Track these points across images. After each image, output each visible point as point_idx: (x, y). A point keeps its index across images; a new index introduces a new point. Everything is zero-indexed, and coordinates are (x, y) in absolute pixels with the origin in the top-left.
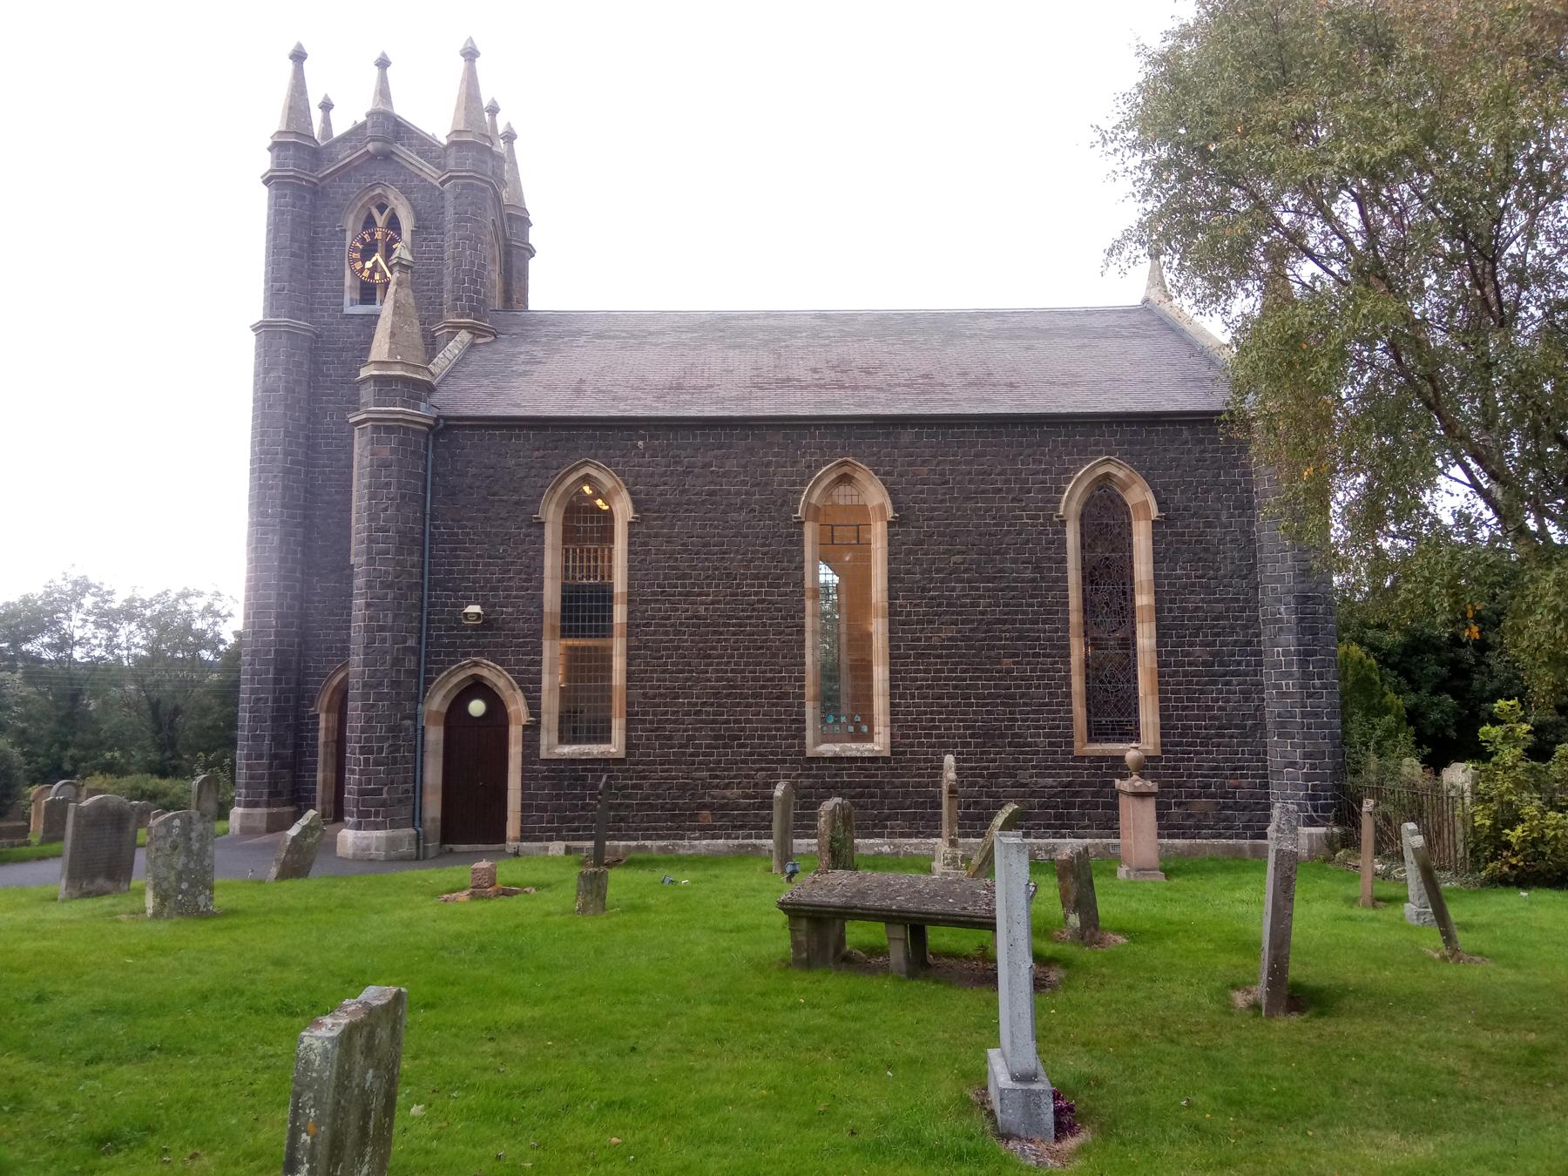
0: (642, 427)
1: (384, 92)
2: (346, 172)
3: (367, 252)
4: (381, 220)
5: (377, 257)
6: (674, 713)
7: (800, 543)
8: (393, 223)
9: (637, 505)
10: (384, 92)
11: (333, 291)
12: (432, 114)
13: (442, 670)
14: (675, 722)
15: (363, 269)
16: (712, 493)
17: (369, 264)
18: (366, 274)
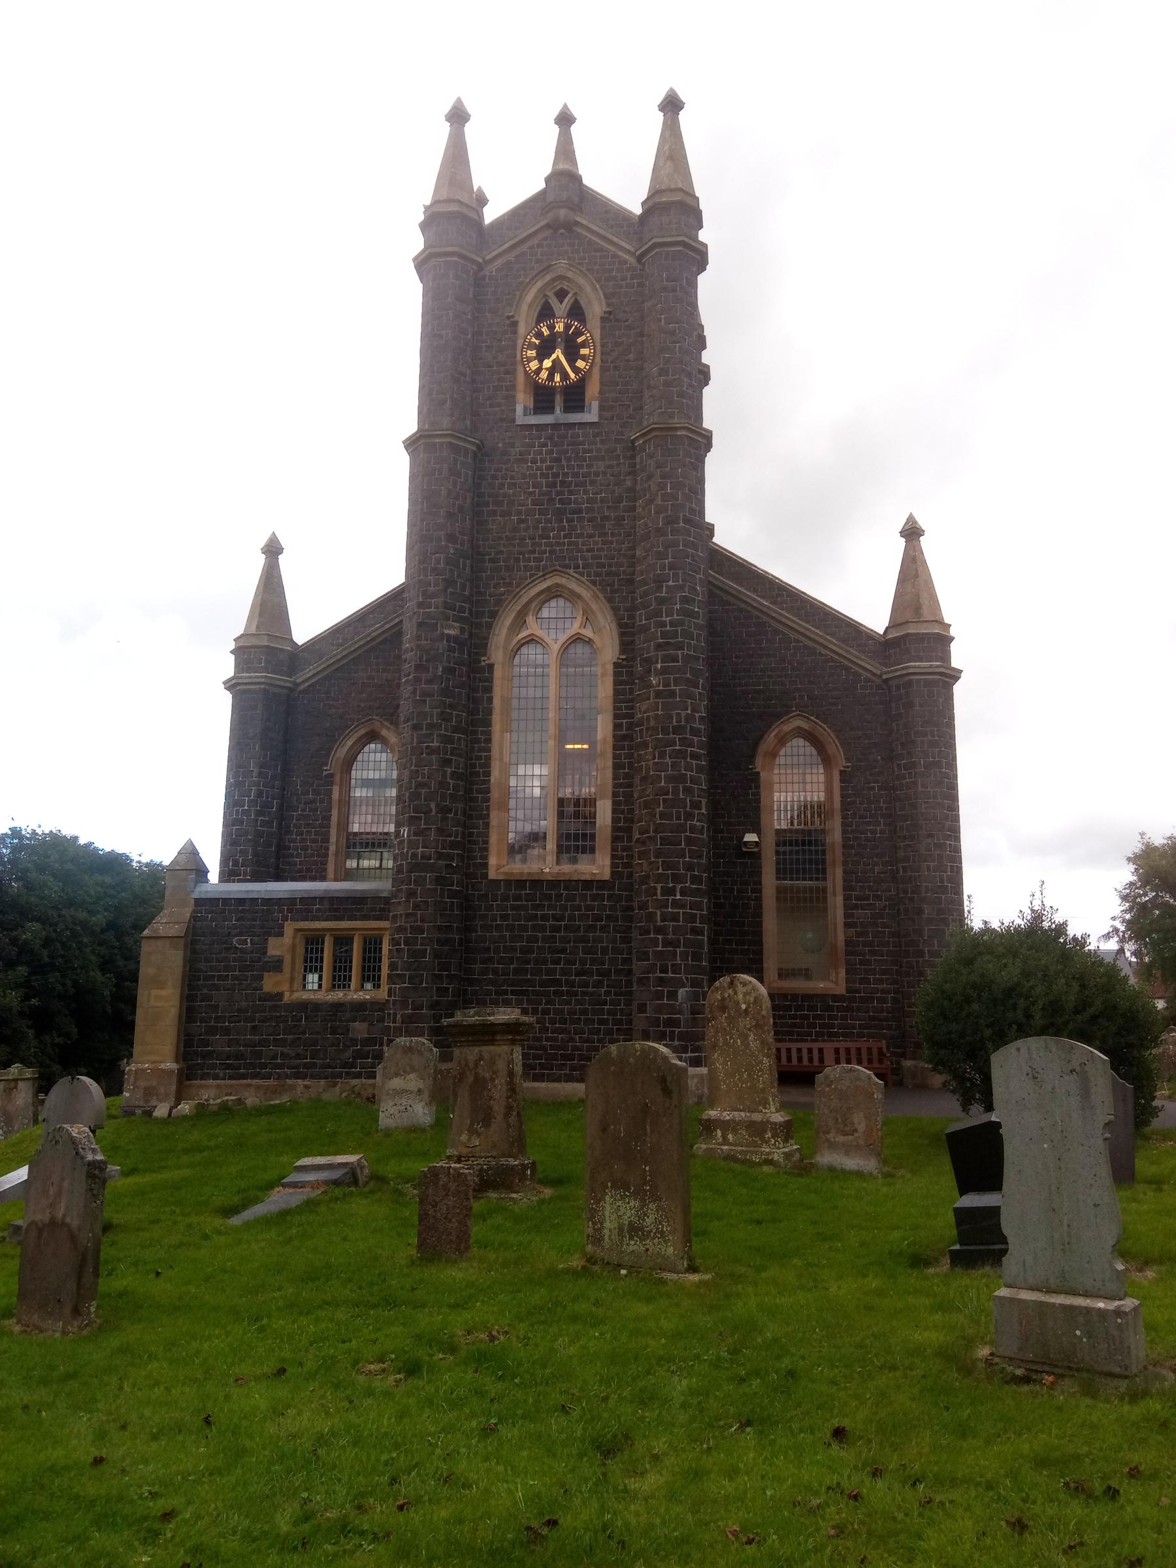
1: (565, 149)
3: (544, 350)
4: (561, 308)
5: (558, 354)
8: (576, 312)
10: (565, 149)
12: (620, 177)
15: (540, 369)
17: (547, 363)
18: (544, 375)
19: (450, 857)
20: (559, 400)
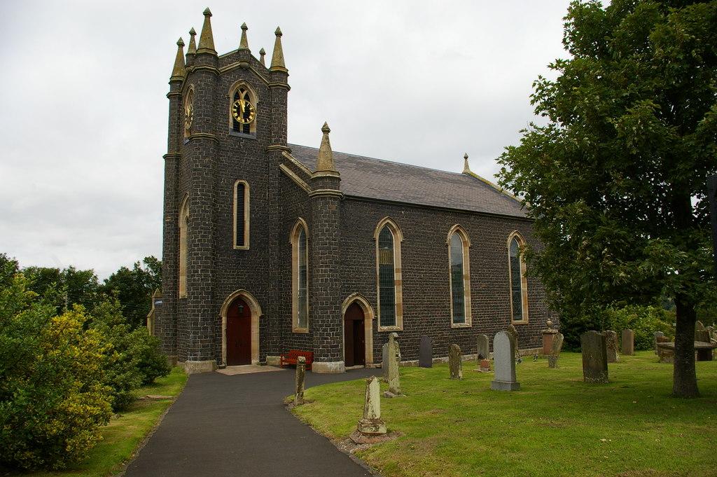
0: (403, 206)
1: (244, 39)
2: (229, 72)
4: (243, 95)
6: (416, 314)
7: (447, 253)
9: (404, 235)
10: (244, 39)
11: (224, 124)
13: (345, 298)
14: (416, 317)
16: (424, 233)
19: (169, 292)
20: (242, 129)
